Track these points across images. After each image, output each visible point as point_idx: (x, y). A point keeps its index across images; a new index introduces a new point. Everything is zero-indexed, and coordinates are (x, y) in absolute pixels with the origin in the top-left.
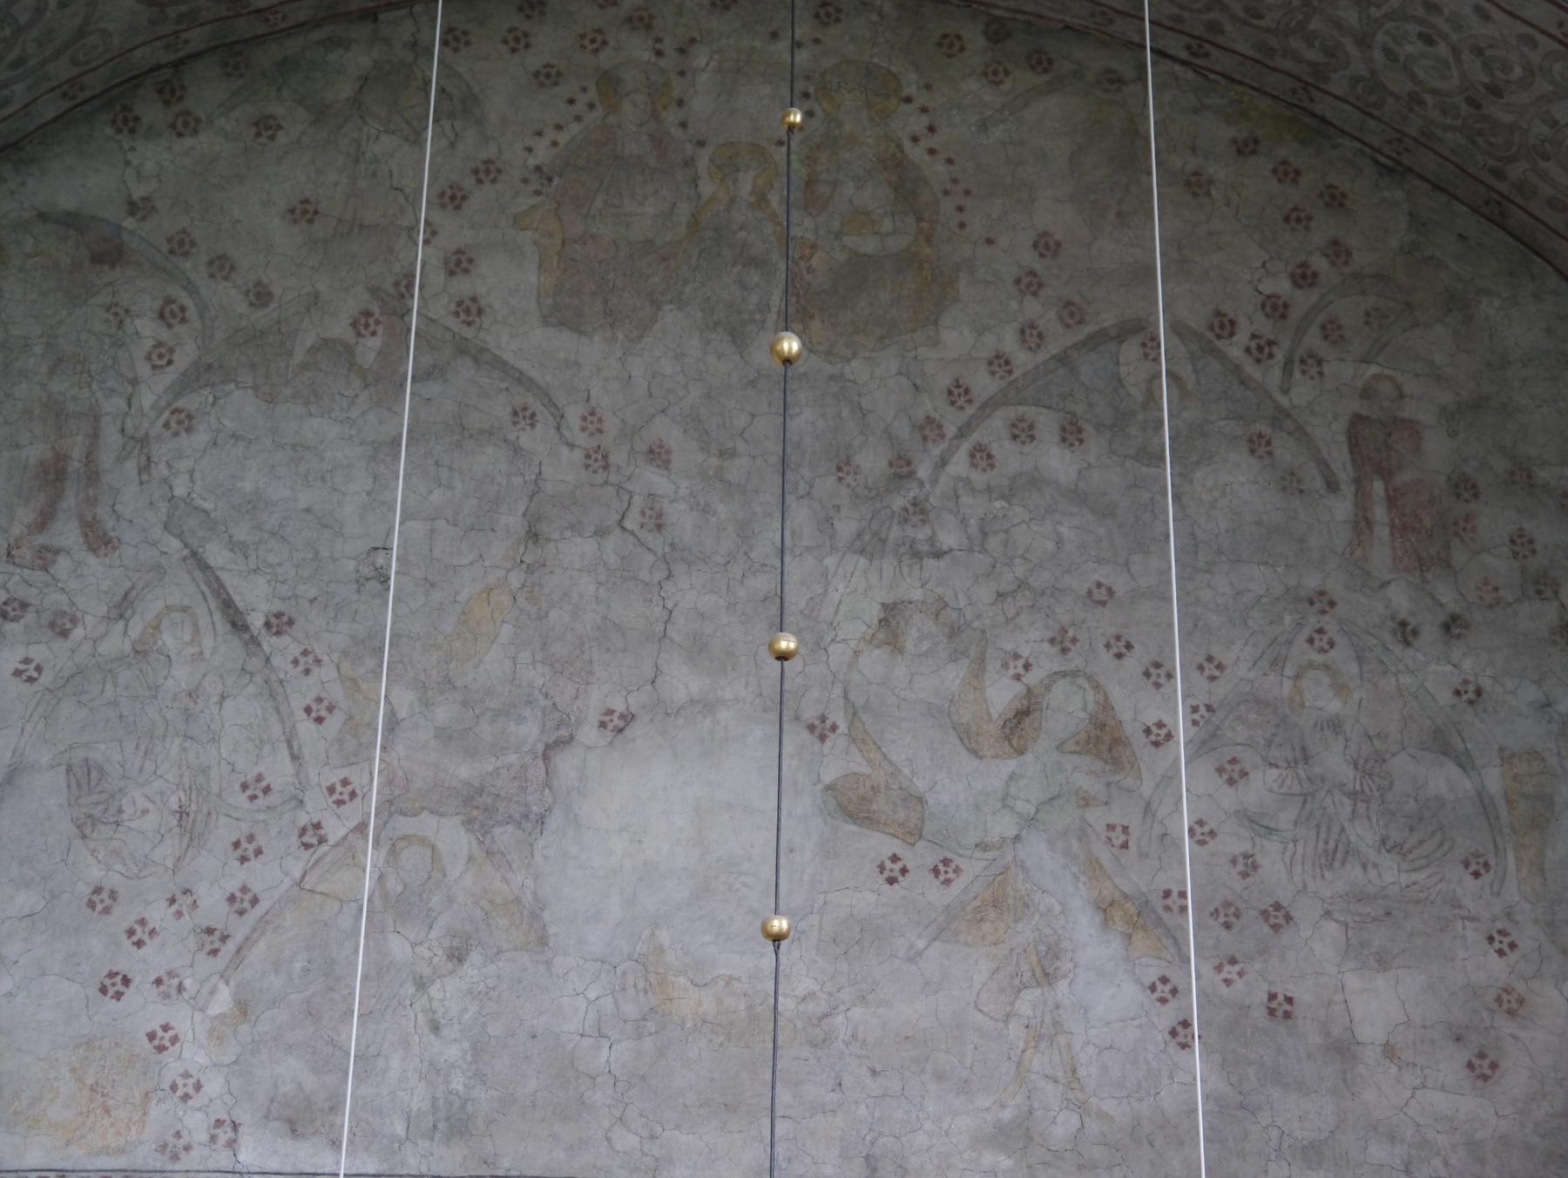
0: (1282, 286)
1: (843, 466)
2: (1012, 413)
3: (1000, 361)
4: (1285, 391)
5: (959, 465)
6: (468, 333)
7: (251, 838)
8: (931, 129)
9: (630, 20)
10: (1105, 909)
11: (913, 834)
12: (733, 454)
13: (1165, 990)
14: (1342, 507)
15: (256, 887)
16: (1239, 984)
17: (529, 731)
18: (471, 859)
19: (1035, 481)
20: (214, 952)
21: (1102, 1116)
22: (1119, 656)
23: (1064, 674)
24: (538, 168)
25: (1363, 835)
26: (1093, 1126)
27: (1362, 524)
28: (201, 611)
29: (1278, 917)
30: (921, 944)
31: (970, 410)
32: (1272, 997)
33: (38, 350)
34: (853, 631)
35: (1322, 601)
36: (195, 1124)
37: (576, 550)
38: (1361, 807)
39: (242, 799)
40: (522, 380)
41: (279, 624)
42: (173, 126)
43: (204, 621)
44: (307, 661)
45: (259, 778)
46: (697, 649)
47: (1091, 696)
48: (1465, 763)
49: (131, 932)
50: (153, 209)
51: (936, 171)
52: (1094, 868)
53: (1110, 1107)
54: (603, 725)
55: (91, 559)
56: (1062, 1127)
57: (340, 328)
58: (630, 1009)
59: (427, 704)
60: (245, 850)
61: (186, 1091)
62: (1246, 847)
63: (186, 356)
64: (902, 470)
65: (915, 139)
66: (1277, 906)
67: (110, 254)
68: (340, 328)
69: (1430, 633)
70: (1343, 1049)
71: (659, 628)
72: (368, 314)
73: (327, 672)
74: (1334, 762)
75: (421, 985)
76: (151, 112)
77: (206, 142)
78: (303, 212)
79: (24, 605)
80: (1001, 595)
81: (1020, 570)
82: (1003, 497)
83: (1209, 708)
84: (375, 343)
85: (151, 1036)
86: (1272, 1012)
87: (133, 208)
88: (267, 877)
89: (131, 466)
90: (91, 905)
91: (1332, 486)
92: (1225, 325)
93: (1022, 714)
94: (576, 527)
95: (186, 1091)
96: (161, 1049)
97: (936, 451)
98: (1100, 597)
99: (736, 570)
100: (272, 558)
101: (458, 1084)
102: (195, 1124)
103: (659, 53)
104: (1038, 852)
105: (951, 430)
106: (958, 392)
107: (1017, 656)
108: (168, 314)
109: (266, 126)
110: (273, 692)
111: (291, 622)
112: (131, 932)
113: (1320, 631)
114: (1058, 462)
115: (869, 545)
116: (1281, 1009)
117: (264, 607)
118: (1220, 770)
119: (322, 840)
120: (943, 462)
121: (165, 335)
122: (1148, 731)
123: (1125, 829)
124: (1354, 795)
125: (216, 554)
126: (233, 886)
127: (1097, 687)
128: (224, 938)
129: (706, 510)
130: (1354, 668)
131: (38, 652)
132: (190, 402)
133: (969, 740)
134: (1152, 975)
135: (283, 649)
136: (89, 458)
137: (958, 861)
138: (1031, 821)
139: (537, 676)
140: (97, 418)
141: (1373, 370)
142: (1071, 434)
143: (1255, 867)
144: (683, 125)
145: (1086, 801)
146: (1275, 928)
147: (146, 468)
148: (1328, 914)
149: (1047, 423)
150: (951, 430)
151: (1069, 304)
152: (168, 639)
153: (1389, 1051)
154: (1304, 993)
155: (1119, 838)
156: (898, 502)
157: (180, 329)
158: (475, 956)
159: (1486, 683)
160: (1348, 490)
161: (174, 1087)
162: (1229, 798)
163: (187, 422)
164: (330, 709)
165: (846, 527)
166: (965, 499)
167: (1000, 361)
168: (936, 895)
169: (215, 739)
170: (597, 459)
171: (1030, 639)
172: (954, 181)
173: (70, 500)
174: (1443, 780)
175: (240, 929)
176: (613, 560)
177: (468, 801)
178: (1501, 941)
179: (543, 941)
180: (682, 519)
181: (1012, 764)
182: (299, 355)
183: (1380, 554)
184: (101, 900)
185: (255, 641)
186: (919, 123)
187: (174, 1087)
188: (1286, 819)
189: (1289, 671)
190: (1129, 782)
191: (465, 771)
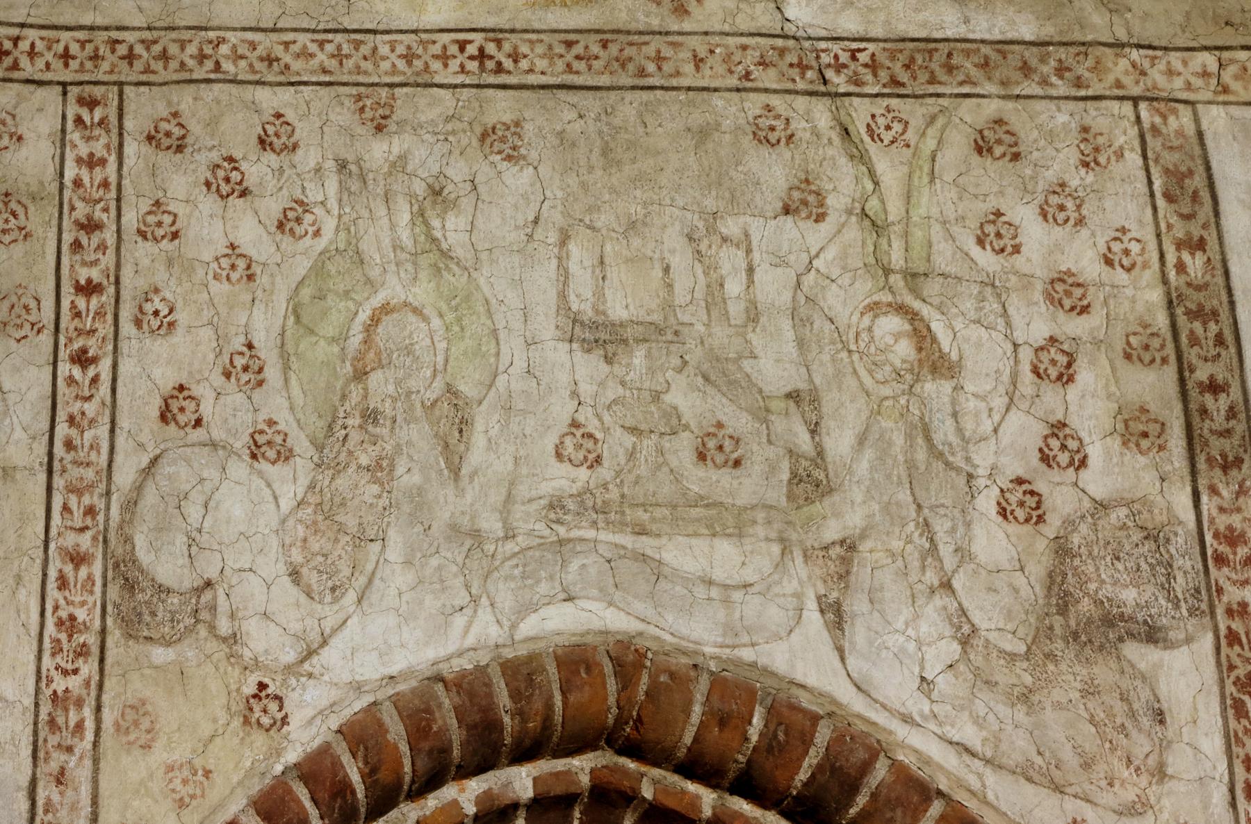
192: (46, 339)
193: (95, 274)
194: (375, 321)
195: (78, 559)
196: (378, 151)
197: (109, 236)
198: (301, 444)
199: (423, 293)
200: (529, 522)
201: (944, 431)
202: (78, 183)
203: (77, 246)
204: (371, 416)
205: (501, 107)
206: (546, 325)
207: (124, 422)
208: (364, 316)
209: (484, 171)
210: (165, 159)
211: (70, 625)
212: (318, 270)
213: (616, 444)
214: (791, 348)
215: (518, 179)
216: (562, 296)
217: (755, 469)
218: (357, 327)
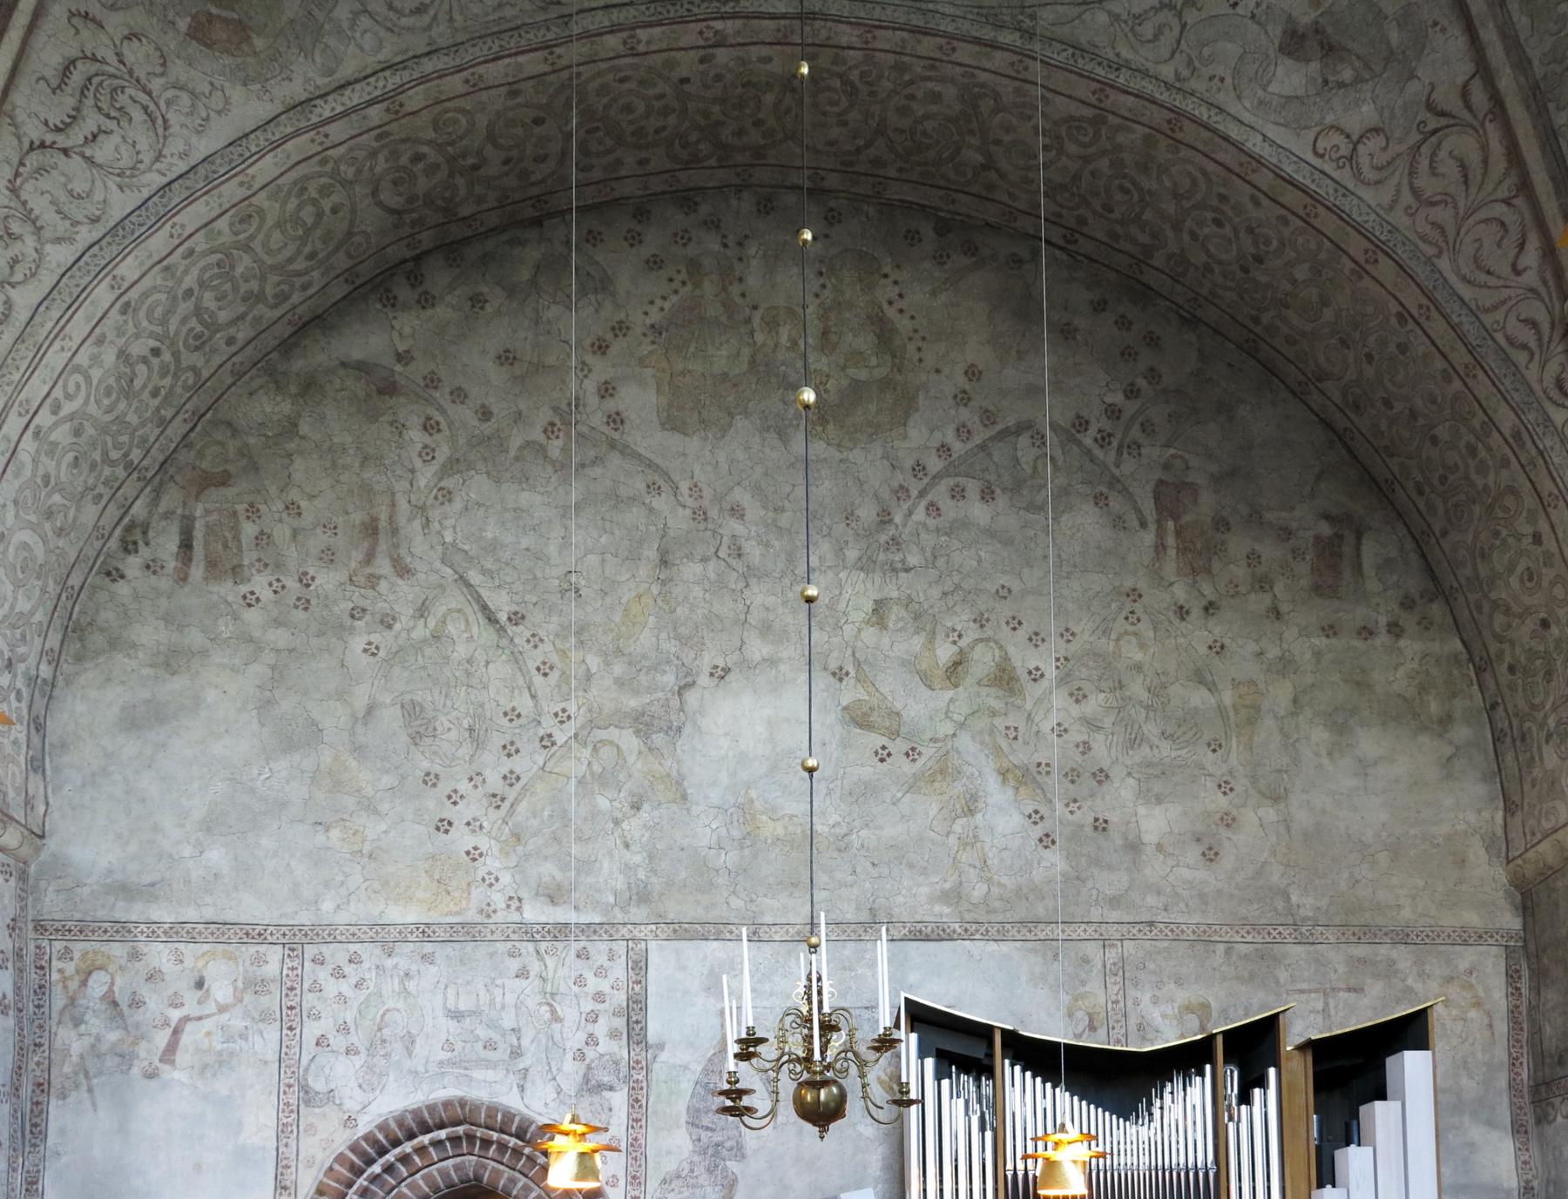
0: (1117, 398)
1: (849, 516)
2: (951, 482)
3: (944, 449)
4: (1118, 466)
5: (920, 514)
6: (616, 436)
7: (512, 743)
8: (901, 296)
9: (705, 222)
10: (1003, 774)
11: (894, 734)
12: (783, 510)
13: (1035, 817)
14: (1149, 538)
15: (518, 771)
16: (1078, 813)
17: (669, 679)
18: (640, 753)
19: (965, 524)
20: (498, 807)
21: (1000, 885)
22: (1014, 629)
23: (981, 640)
24: (653, 326)
25: (1151, 730)
26: (995, 890)
27: (1160, 547)
28: (469, 611)
29: (1102, 776)
30: (899, 795)
31: (926, 480)
32: (1096, 820)
33: (351, 452)
34: (857, 617)
35: (1135, 594)
36: (498, 900)
37: (691, 570)
38: (1151, 714)
39: (505, 721)
40: (651, 465)
41: (516, 618)
42: (418, 302)
43: (471, 618)
44: (535, 640)
45: (514, 709)
46: (766, 629)
47: (997, 652)
48: (1212, 687)
49: (449, 797)
50: (412, 358)
51: (904, 324)
52: (997, 751)
53: (1005, 880)
54: (712, 675)
55: (400, 582)
56: (979, 891)
57: (537, 435)
58: (736, 833)
59: (608, 664)
60: (510, 750)
61: (491, 882)
62: (1085, 737)
63: (443, 453)
64: (885, 519)
65: (890, 303)
66: (1101, 770)
67: (390, 389)
68: (537, 435)
69: (1196, 612)
70: (1134, 847)
71: (742, 617)
72: (553, 424)
73: (547, 647)
74: (1137, 689)
75: (617, 822)
76: (404, 292)
77: (441, 312)
78: (506, 358)
79: (364, 610)
80: (945, 594)
81: (956, 578)
82: (946, 534)
83: (1066, 659)
84: (559, 443)
85: (468, 853)
86: (1096, 828)
87: (400, 357)
88: (519, 764)
89: (417, 524)
90: (425, 782)
91: (1143, 525)
92: (1082, 424)
93: (957, 664)
94: (690, 557)
95: (491, 882)
96: (474, 860)
97: (905, 506)
98: (1003, 594)
99: (787, 581)
100: (508, 579)
101: (642, 875)
102: (498, 900)
103: (725, 246)
104: (965, 742)
105: (914, 493)
106: (919, 469)
107: (954, 630)
108: (429, 427)
109: (477, 300)
110: (517, 659)
111: (523, 617)
112: (449, 797)
113: (1133, 612)
114: (979, 512)
115: (866, 565)
116: (1101, 826)
117: (506, 608)
118: (1071, 695)
119: (553, 744)
120: (910, 513)
121: (428, 440)
122: (1030, 673)
123: (1016, 728)
124: (1148, 708)
125: (474, 577)
126: (505, 771)
127: (1001, 648)
128: (503, 799)
129: (767, 545)
130: (1151, 634)
131: (375, 638)
132: (448, 483)
133: (926, 680)
134: (1030, 810)
135: (520, 633)
136: (391, 519)
137: (920, 749)
138: (962, 725)
139: (671, 647)
140: (393, 494)
141: (1172, 451)
142: (987, 495)
143: (1090, 749)
144: (743, 295)
145: (994, 714)
146: (1100, 782)
147: (427, 523)
148: (1129, 774)
149: (973, 488)
150: (914, 493)
151: (987, 411)
152: (451, 629)
153: (1160, 847)
154: (1114, 818)
155: (1012, 734)
156: (883, 538)
157: (437, 436)
158: (646, 807)
159: (1227, 642)
160: (1153, 527)
161: (483, 880)
162: (1075, 710)
163: (447, 496)
164: (551, 668)
165: (852, 554)
166: (923, 535)
167: (944, 449)
168: (908, 768)
169: (486, 687)
170: (700, 515)
171: (961, 619)
172: (916, 331)
173: (383, 546)
174: (1199, 698)
175: (511, 794)
176: (713, 576)
177: (636, 719)
178: (1225, 787)
179: (684, 797)
180: (754, 551)
181: (951, 693)
182: (512, 453)
183: (1170, 568)
184: (430, 780)
185: (502, 629)
186: (892, 292)
187: (483, 880)
188: (1108, 722)
189: (1113, 636)
190: (1019, 702)
191: (633, 703)
192: (278, 1023)
193: (293, 1004)
194: (384, 1014)
195: (290, 1086)
196: (389, 963)
197: (298, 991)
198: (362, 1049)
199: (401, 1005)
200: (433, 1068)
201: (557, 1037)
202: (288, 975)
203: (287, 995)
204: (384, 1041)
205: (429, 948)
206: (440, 1013)
207: (304, 1047)
208: (381, 1013)
209: (422, 968)
210: (318, 967)
211: (288, 1104)
212: (367, 1000)
213: (459, 1046)
214: (513, 1017)
215: (433, 969)
216: (445, 1004)
217: (500, 1050)
218: (378, 1016)
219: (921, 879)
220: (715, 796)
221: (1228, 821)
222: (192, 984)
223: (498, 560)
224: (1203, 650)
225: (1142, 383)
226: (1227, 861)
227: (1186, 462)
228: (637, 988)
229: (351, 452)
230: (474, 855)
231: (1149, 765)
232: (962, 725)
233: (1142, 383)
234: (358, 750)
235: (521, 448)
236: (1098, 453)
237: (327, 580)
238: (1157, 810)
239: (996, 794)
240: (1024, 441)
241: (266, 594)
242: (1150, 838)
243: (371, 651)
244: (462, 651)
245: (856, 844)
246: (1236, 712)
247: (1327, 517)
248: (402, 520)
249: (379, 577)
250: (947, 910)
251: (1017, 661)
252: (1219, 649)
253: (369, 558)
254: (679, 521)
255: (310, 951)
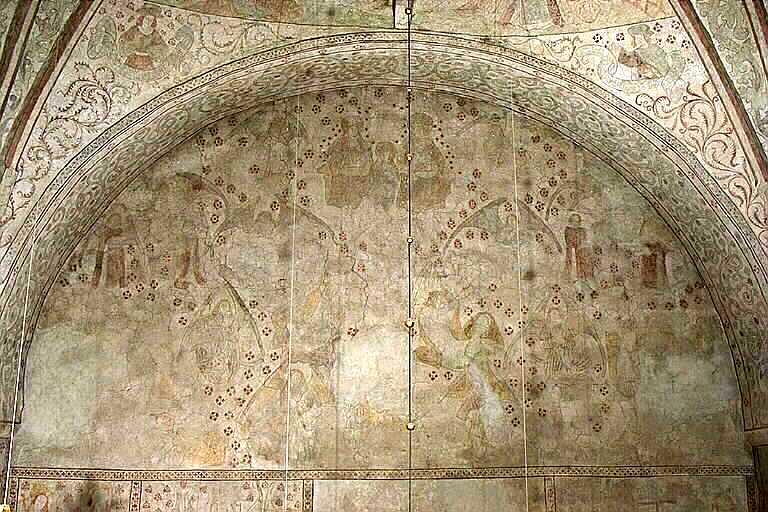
4: (547, 220)
8: (442, 136)
10: (493, 386)
13: (509, 409)
14: (563, 258)
27: (569, 262)
36: (240, 456)
41: (254, 304)
44: (263, 315)
46: (375, 309)
52: (490, 374)
53: (494, 444)
57: (267, 209)
59: (297, 328)
63: (222, 219)
65: (437, 139)
67: (198, 186)
68: (267, 209)
73: (268, 319)
78: (254, 169)
91: (560, 251)
97: (445, 242)
105: (449, 235)
110: (253, 325)
127: (492, 318)
128: (244, 401)
130: (565, 309)
135: (255, 312)
142: (484, 236)
145: (489, 354)
150: (449, 235)
156: (434, 259)
158: (315, 406)
160: (565, 251)
168: (445, 383)
170: (344, 249)
171: (473, 303)
175: (248, 399)
181: (467, 342)
183: (574, 273)
184: (209, 391)
191: (308, 349)
196: (184, 491)
205: (204, 484)
215: (205, 496)
219: (452, 444)
220: (349, 399)
221: (606, 409)
222: (86, 503)
223: (246, 274)
224: (591, 317)
225: (557, 178)
226: (606, 431)
227: (580, 217)
228: (308, 507)
229: (179, 218)
230: (228, 432)
231: (567, 379)
232: (473, 360)
233: (557, 178)
234: (174, 375)
235: (260, 215)
236: (538, 214)
237: (163, 285)
238: (571, 404)
239: (491, 397)
240: (502, 208)
241: (134, 293)
242: (567, 419)
243: (182, 321)
244: (227, 322)
245: (420, 426)
246: (608, 350)
247: (649, 246)
248: (200, 253)
249: (189, 283)
250: (465, 462)
251: (499, 323)
252: (599, 316)
253: (184, 274)
254: (335, 253)
255: (145, 485)
